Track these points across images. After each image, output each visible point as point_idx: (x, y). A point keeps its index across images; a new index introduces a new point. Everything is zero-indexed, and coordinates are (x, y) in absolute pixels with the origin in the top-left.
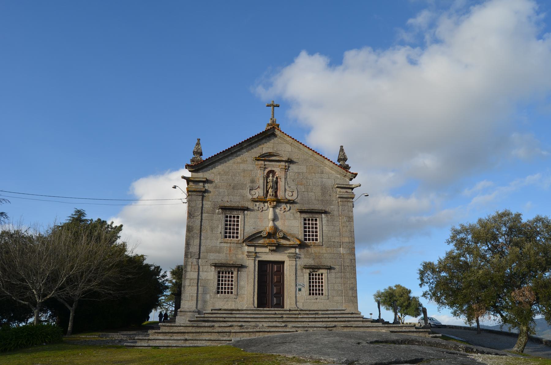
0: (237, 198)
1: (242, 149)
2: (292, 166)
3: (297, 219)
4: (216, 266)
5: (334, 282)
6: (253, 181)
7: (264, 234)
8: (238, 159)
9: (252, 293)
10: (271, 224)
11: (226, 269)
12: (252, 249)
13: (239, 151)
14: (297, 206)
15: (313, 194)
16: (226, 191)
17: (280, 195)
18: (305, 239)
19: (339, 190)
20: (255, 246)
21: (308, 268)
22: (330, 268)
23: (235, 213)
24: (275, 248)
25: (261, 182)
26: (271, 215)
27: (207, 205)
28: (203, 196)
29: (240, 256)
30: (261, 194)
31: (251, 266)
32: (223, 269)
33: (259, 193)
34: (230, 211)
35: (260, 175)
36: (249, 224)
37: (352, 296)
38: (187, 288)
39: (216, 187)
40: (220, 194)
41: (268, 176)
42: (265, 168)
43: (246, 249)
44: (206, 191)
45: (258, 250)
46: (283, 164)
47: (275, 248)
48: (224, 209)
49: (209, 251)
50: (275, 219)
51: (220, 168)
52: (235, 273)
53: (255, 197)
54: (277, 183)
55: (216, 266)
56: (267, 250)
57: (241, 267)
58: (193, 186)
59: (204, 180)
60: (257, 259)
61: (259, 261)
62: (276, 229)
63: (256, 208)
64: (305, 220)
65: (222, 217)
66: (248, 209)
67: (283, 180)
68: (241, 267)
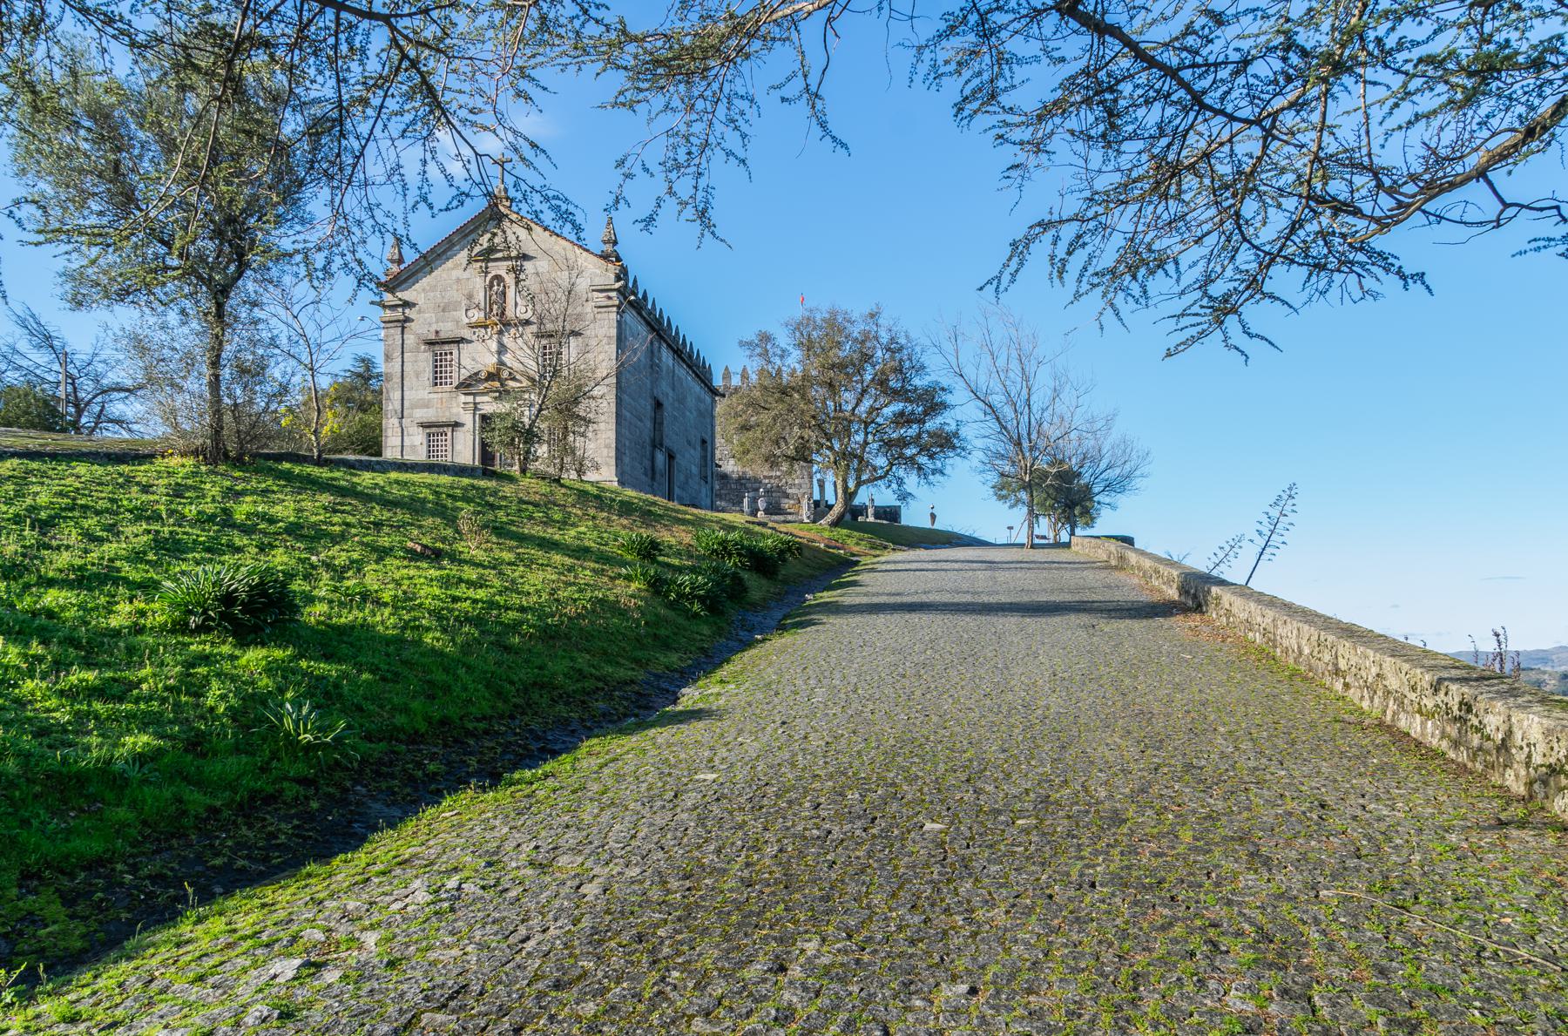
1: (454, 245)
2: (528, 265)
4: (424, 426)
6: (470, 297)
7: (483, 375)
8: (450, 264)
10: (494, 360)
11: (436, 429)
12: (470, 399)
13: (449, 249)
17: (510, 313)
19: (596, 294)
23: (446, 347)
25: (480, 297)
26: (494, 346)
27: (410, 339)
28: (403, 328)
29: (454, 410)
30: (482, 314)
32: (433, 430)
33: (477, 316)
35: (478, 284)
39: (419, 312)
40: (424, 323)
41: (491, 286)
42: (487, 273)
43: (463, 398)
44: (407, 320)
45: (478, 399)
48: (431, 343)
49: (413, 407)
50: (502, 349)
51: (425, 282)
54: (504, 293)
55: (424, 426)
56: (486, 398)
57: (456, 425)
58: (389, 314)
62: (501, 363)
63: (474, 338)
65: (429, 355)
66: (462, 340)
67: (513, 287)
68: (456, 425)
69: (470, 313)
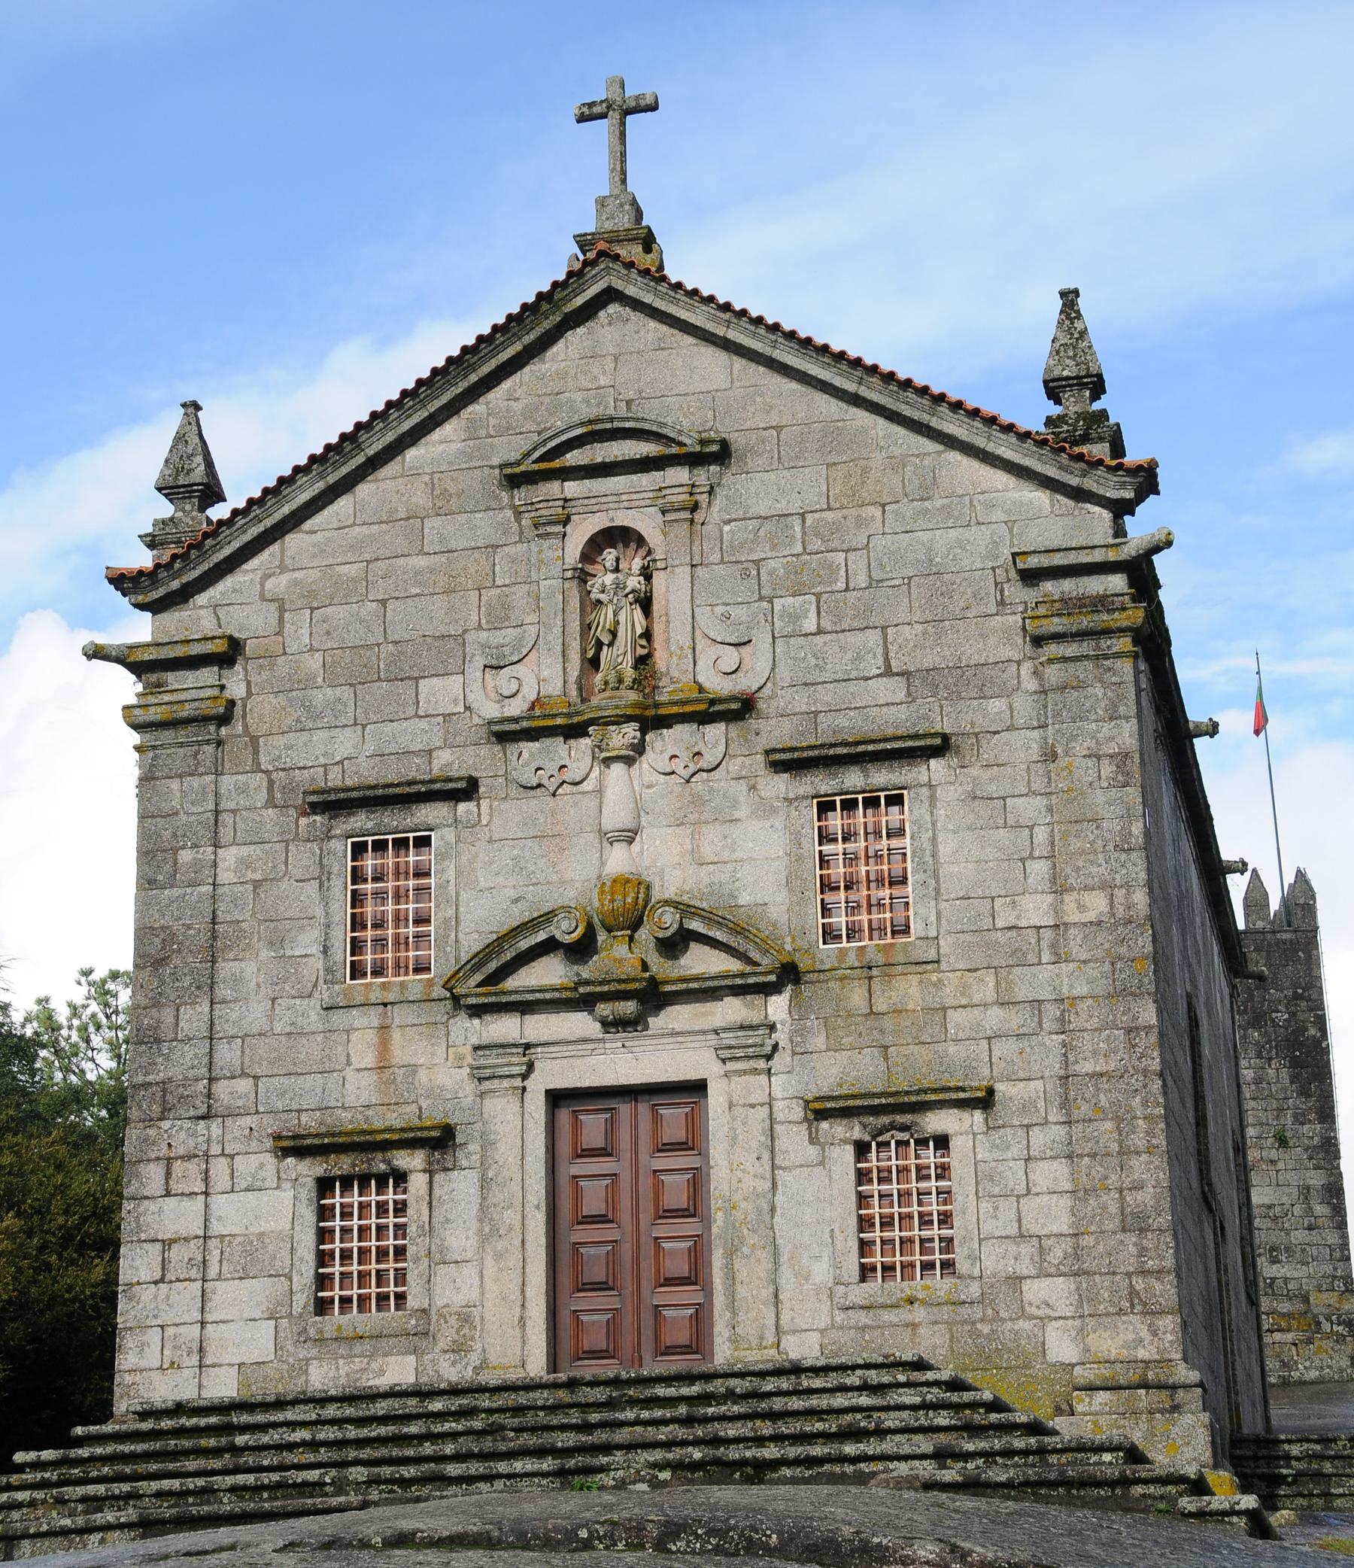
0: (414, 734)
3: (774, 810)
5: (1021, 1189)
9: (516, 1296)
11: (356, 1161)
14: (774, 730)
15: (874, 637)
16: (346, 693)
18: (829, 934)
20: (524, 1008)
21: (846, 1113)
22: (985, 1101)
24: (629, 1007)
31: (513, 1133)
34: (380, 812)
36: (484, 878)
37: (1144, 1273)
38: (147, 1294)
45: (539, 1027)
46: (679, 475)
47: (629, 1007)
52: (417, 1182)
53: (516, 708)
59: (219, 647)
60: (538, 1085)
61: (556, 1098)
64: (825, 808)
69: (504, 681)
